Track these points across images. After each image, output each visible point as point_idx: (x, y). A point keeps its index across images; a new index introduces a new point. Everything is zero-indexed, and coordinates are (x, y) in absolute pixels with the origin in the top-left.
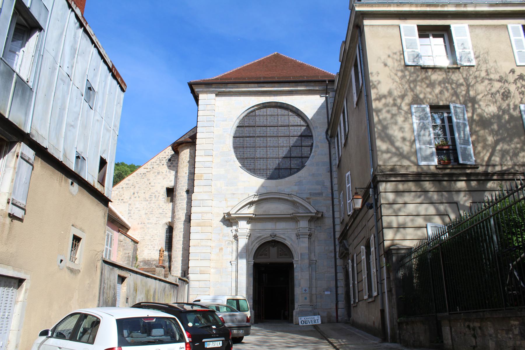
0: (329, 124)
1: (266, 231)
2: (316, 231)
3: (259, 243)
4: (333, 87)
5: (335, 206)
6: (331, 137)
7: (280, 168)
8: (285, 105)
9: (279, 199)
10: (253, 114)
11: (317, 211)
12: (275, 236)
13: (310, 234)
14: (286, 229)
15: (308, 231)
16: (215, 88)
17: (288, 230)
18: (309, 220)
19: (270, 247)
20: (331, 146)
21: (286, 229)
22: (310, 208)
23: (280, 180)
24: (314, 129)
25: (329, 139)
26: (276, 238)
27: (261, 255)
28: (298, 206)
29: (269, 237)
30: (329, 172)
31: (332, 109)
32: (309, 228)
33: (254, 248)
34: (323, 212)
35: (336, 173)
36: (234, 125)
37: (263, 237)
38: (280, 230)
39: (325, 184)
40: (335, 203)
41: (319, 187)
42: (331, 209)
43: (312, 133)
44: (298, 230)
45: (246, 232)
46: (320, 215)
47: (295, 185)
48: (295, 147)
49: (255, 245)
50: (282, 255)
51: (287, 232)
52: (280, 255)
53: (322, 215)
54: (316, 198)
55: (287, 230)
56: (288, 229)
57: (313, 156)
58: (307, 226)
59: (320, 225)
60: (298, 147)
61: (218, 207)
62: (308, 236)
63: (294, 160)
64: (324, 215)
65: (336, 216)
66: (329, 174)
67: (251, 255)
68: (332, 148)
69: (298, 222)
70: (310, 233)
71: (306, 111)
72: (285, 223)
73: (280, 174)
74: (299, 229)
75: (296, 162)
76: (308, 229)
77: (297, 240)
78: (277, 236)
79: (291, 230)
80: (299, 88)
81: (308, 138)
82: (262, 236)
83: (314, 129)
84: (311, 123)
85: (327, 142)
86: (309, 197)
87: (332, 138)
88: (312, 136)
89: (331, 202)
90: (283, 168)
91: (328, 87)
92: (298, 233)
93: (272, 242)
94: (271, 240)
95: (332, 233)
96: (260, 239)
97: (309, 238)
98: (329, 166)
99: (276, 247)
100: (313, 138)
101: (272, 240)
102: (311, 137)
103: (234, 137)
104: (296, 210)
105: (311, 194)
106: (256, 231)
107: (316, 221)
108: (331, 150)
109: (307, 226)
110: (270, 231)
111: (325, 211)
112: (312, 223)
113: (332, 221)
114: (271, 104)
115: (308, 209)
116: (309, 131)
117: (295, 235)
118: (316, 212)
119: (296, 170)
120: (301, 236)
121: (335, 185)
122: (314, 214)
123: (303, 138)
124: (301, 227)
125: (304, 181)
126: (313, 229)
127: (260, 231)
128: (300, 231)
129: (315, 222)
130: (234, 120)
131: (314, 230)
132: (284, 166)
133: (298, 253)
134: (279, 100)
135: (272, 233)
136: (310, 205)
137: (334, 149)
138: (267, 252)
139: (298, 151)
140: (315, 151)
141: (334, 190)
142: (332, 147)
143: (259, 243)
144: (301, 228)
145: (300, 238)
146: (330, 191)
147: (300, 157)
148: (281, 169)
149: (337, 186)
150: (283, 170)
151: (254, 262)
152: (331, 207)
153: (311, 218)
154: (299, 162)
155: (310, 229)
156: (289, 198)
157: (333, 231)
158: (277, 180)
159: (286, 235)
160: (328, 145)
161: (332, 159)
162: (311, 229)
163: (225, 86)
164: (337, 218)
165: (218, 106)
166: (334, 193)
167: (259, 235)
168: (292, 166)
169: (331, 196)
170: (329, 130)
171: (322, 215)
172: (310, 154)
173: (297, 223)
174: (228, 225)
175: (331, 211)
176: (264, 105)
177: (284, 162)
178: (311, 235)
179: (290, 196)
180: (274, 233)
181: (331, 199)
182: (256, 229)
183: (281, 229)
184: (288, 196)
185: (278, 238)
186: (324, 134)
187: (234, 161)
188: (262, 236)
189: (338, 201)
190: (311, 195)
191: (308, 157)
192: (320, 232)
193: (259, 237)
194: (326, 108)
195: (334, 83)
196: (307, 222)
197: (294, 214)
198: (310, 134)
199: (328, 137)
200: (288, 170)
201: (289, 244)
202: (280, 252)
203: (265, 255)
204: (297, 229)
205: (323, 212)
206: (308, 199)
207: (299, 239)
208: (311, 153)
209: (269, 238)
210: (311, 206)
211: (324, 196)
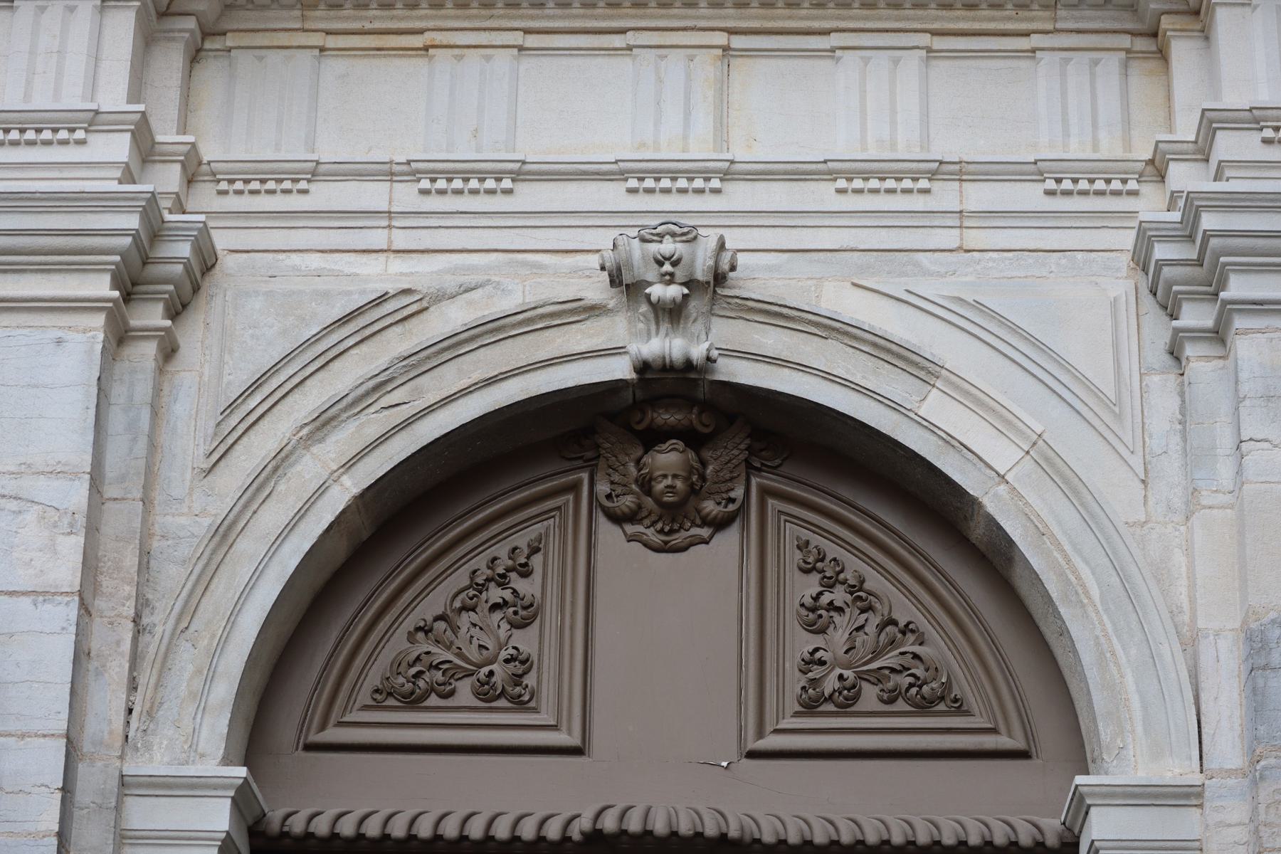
1: (531, 196)
3: (372, 424)
17: (980, 196)
19: (608, 533)
27: (413, 701)
33: (272, 516)
38: (822, 195)
44: (1183, 177)
49: (280, 462)
50: (847, 700)
51: (949, 238)
52: (810, 706)
55: (946, 196)
56: (960, 172)
67: (187, 660)
69: (1182, 51)
74: (1202, 151)
79: (1030, 196)
82: (441, 297)
93: (652, 438)
94: (620, 369)
96: (399, 343)
99: (728, 540)
106: (325, 195)
110: (612, 196)
120: (1238, 288)
124: (1234, 98)
127: (406, 196)
133: (1190, 644)
138: (525, 641)
143: (372, 424)
145: (1218, 335)
151: (242, 800)
159: (928, 288)
173: (1162, 55)
174: (97, 675)
185: (771, 340)
188: (441, 297)
201: (1001, 454)
202: (805, 642)
203: (487, 694)
204: (1157, 169)
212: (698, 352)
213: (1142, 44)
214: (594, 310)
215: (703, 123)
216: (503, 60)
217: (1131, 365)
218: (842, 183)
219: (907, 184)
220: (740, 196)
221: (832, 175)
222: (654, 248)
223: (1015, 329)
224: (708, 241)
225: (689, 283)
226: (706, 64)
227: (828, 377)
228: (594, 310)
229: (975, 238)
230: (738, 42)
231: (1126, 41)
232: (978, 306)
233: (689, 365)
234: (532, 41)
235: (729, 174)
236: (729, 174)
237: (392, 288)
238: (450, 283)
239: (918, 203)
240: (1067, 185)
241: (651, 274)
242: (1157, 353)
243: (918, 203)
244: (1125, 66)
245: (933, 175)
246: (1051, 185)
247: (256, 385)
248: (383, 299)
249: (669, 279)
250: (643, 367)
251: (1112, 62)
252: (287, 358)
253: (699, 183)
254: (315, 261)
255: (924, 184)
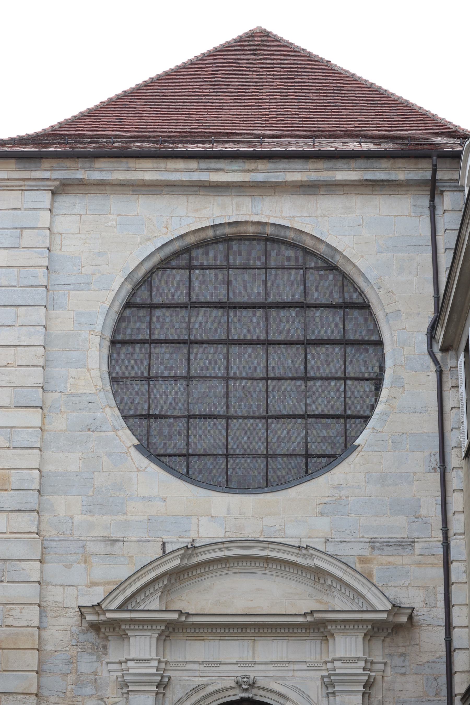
0: (439, 310)
2: (388, 669)
4: (456, 177)
5: (453, 588)
6: (445, 349)
7: (270, 452)
8: (290, 235)
9: (267, 559)
10: (183, 261)
11: (394, 605)
12: (253, 685)
13: (367, 681)
14: (289, 663)
15: (360, 671)
16: (52, 169)
17: (296, 667)
18: (366, 635)
20: (445, 379)
21: (289, 663)
22: (369, 596)
23: (270, 497)
24: (388, 321)
25: (439, 355)
26: (255, 691)
28: (330, 586)
29: (231, 688)
30: (435, 469)
31: (448, 271)
32: (366, 661)
34: (413, 609)
35: (461, 473)
36: (114, 300)
37: (211, 689)
38: (270, 667)
39: (423, 512)
40: (453, 578)
41: (402, 521)
42: (441, 596)
43: (379, 333)
45: (154, 671)
46: (404, 619)
47: (322, 514)
48: (324, 382)
51: (291, 674)
53: (411, 617)
54: (392, 559)
55: (291, 667)
56: (293, 663)
57: (383, 413)
58: (360, 655)
59: (401, 650)
60: (333, 382)
61: (61, 586)
62: (361, 688)
63: (319, 426)
64: (416, 618)
65: (455, 621)
66: (437, 476)
68: (447, 386)
69: (331, 641)
70: (369, 677)
71: (362, 257)
72: (285, 642)
73: (270, 473)
75: (324, 433)
76: (362, 664)
77: (325, 699)
78: (259, 684)
79: (304, 667)
80: (340, 176)
81: (367, 350)
82: (208, 685)
83: (388, 321)
84: (379, 297)
85: (433, 367)
86: (366, 553)
87: (451, 353)
88: (379, 343)
89: (442, 571)
90: (279, 452)
91: (439, 175)
92: (329, 677)
94: (237, 698)
95: (444, 679)
96: (202, 694)
97: (364, 694)
98: (437, 450)
100: (383, 349)
101: (243, 700)
102: (379, 347)
103: (113, 342)
104: (325, 599)
105: (372, 544)
106: (188, 667)
107: (389, 634)
108: (445, 394)
109: (360, 655)
110: (236, 667)
111: (422, 604)
112: (377, 646)
113: (444, 636)
114: (242, 229)
115: (363, 597)
116: (370, 326)
117: (319, 683)
118: (389, 607)
119: (324, 460)
120: (337, 688)
121: (457, 516)
122: (384, 616)
123: (351, 350)
124: (338, 656)
125: (351, 500)
126: (379, 662)
127: (202, 667)
128: (334, 669)
129: (388, 640)
130: (116, 286)
131: (382, 666)
132: (284, 446)
134: (269, 217)
135: (242, 677)
136: (369, 585)
137: (455, 390)
139: (333, 394)
140: (391, 398)
141: (451, 533)
142: (448, 384)
144: (340, 659)
145: (334, 693)
146: (440, 535)
147: (338, 417)
148: (275, 456)
149: (461, 517)
150: (279, 459)
152: (441, 590)
153: (373, 628)
154: (333, 433)
155: (369, 665)
156: (300, 560)
157: (445, 671)
158: (261, 496)
159: (288, 683)
160: (433, 377)
161: (448, 425)
162: (372, 662)
163: (88, 165)
164: (459, 627)
165: (61, 234)
166: (452, 544)
167: (198, 681)
168: (314, 448)
169: (440, 551)
170: (439, 328)
171: (411, 617)
172: (373, 407)
173: (327, 640)
175: (442, 604)
176: (218, 233)
177: (284, 433)
178: (373, 682)
179: (304, 551)
180: (249, 677)
181: (441, 562)
182: (187, 663)
183: (271, 663)
184: (297, 551)
185: (262, 693)
186: (423, 338)
187: (115, 430)
188: (208, 685)
189: (464, 569)
190: (373, 548)
191: (366, 418)
192: (404, 674)
193: (196, 689)
194: (430, 248)
195: (459, 162)
196: (361, 639)
197: (316, 615)
198: (376, 338)
199: (436, 348)
200: (300, 459)
205: (414, 608)
206: (363, 560)
207: (331, 698)
208: (376, 401)
209: (231, 692)
210: (373, 588)
211: (417, 551)
212: (251, 696)
213: (324, 638)
214: (233, 688)
215: (251, 653)
216: (217, 642)
217: (320, 696)
218: (274, 665)
219: (284, 665)
220: (257, 667)
221: (272, 664)
222: (243, 680)
223: (301, 691)
224: (252, 678)
225: (249, 685)
226: (251, 643)
227: (271, 699)
228: (233, 688)
229: (296, 674)
230: (256, 638)
231: (321, 638)
232: (295, 687)
233: (249, 697)
234: (222, 638)
235: (255, 663)
236: (255, 663)
237: (200, 684)
238: (210, 682)
239: (286, 668)
240: (311, 665)
241: (242, 684)
242: (325, 694)
243: (286, 668)
244: (321, 642)
245: (288, 664)
246: (308, 665)
247: (179, 701)
248: (199, 686)
249: (246, 685)
250: (242, 698)
251: (319, 642)
252: (184, 696)
253: (250, 665)
254: (187, 678)
255: (287, 665)
